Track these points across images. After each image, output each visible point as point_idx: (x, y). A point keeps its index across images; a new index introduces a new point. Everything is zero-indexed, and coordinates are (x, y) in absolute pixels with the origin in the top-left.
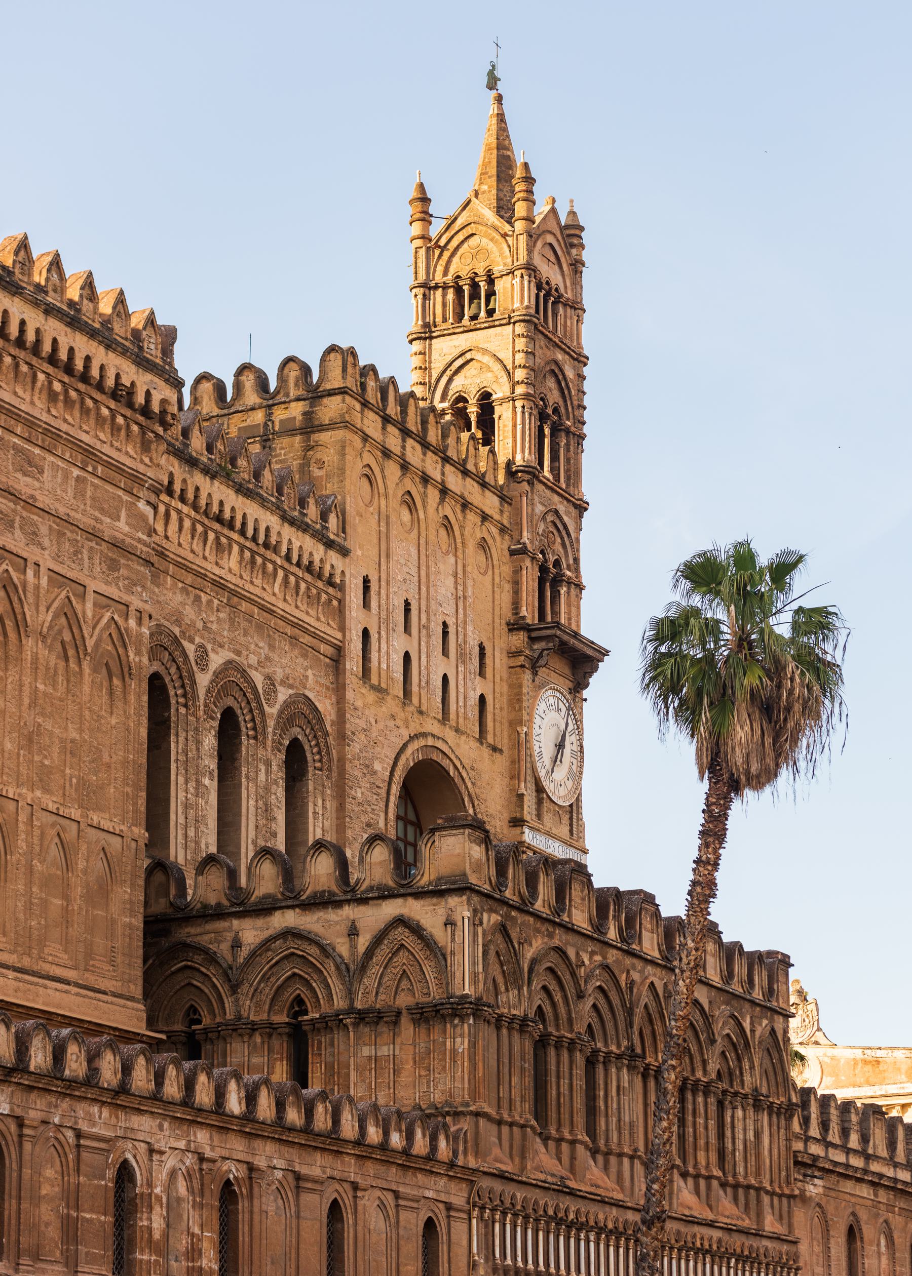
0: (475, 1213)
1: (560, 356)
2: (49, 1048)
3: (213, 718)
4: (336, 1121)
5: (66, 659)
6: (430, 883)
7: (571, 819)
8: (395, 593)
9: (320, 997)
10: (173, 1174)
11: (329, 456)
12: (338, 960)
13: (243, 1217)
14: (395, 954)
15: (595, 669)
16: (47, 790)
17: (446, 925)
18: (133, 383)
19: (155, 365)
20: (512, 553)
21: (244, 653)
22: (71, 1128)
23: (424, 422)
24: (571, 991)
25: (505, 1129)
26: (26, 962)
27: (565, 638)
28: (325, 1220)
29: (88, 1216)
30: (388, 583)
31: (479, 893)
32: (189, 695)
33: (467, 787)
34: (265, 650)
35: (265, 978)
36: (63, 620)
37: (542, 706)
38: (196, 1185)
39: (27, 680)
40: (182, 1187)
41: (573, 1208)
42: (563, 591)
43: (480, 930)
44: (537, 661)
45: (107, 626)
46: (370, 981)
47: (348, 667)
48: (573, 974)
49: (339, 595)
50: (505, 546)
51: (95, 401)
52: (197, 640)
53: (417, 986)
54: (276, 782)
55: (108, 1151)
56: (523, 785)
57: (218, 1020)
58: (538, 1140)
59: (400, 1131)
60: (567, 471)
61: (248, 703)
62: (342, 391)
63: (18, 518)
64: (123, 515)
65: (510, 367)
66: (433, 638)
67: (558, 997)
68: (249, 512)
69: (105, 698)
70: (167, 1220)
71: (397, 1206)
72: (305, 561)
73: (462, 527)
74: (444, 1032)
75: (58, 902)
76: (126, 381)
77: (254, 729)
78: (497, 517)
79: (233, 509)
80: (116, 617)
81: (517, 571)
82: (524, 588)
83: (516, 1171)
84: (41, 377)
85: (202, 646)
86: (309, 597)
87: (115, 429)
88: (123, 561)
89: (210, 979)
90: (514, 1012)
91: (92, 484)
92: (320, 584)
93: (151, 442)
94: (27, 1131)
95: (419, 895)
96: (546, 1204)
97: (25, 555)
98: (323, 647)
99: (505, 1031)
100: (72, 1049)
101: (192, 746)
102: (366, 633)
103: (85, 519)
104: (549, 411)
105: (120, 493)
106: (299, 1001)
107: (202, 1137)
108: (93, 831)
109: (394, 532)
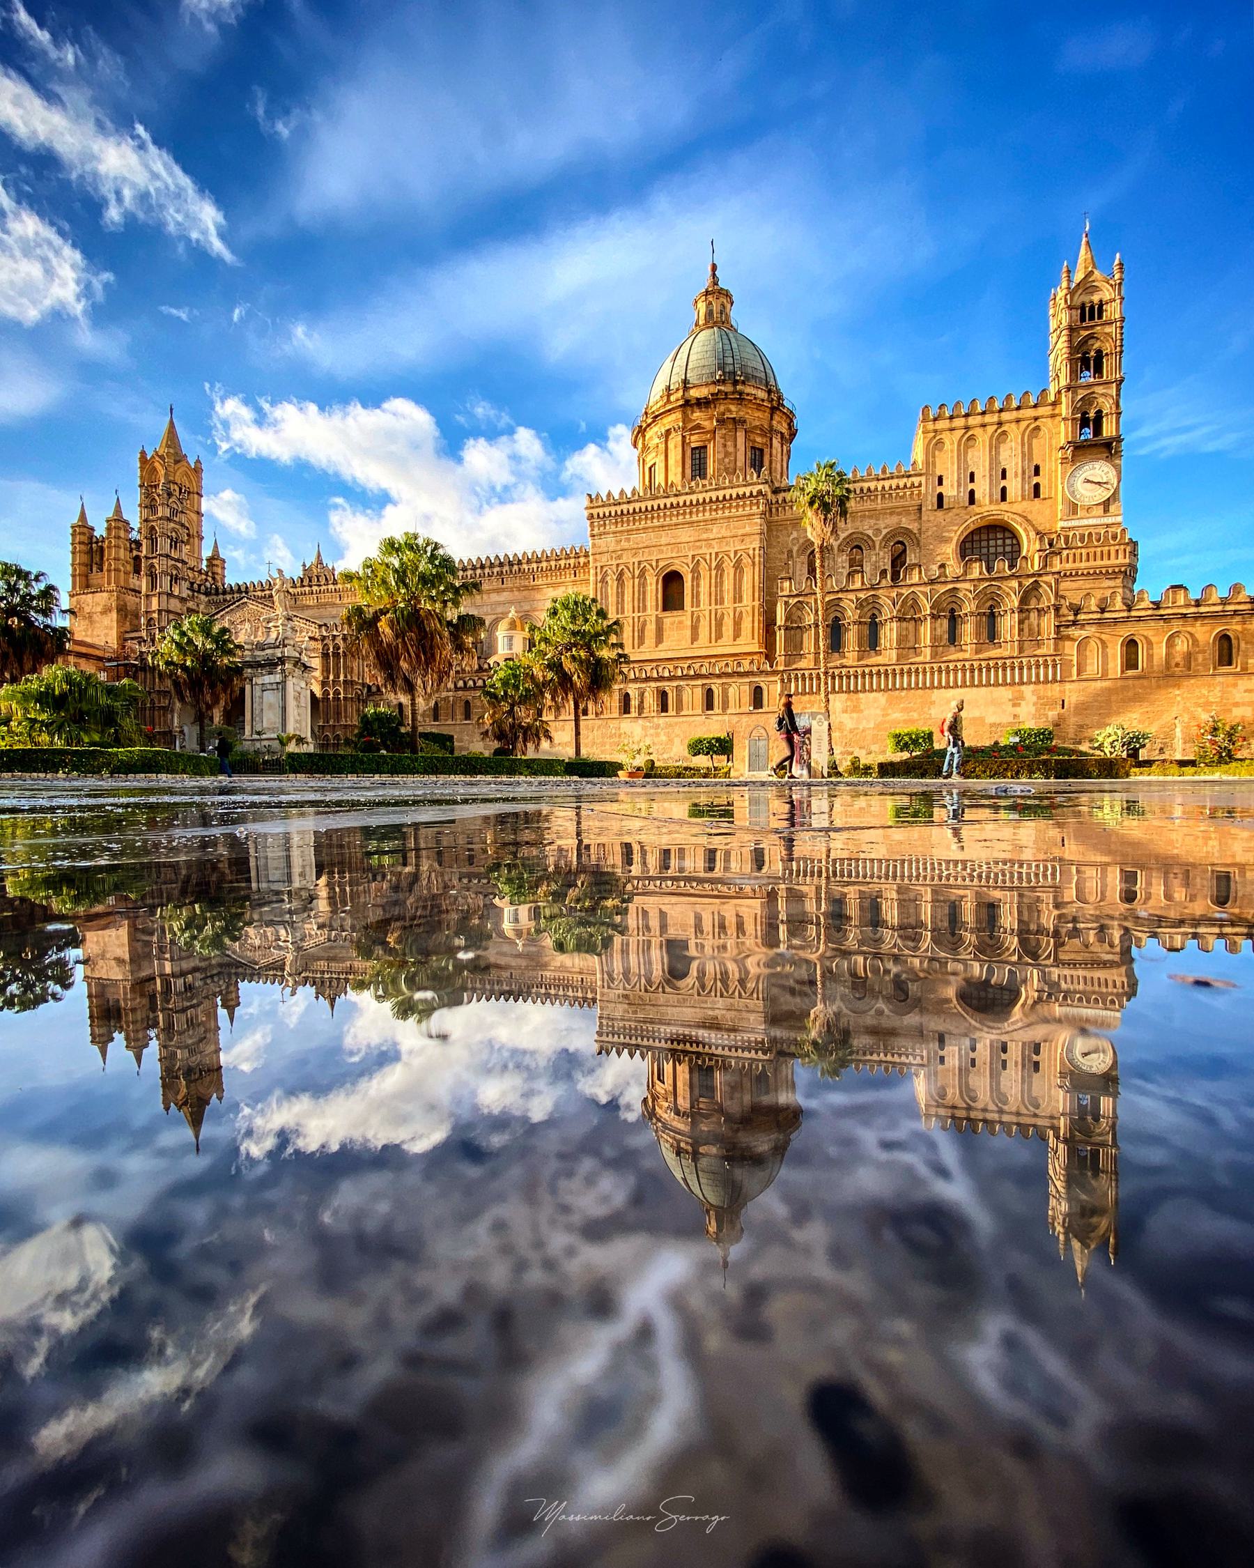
76: (741, 493)
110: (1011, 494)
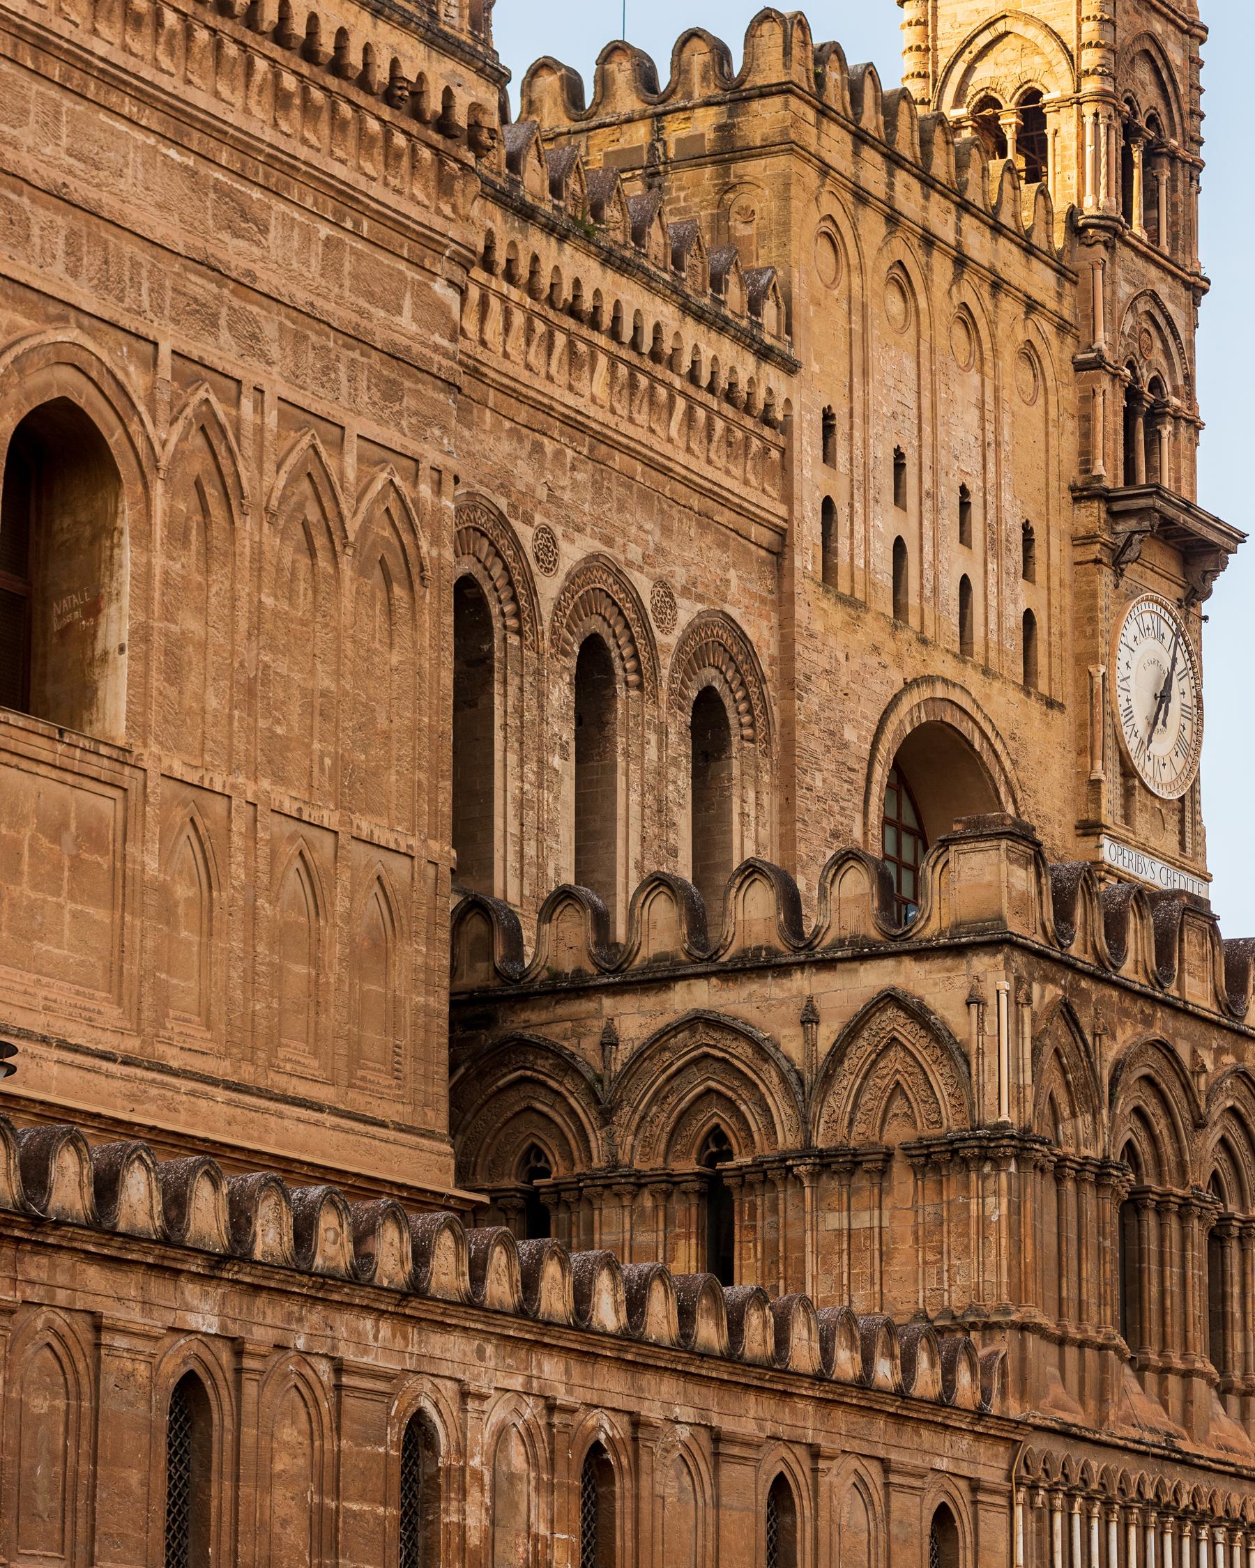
0: (1020, 1496)
1: (1158, 27)
2: (288, 1221)
3: (565, 653)
4: (782, 1341)
5: (312, 553)
6: (941, 934)
7: (1182, 821)
8: (878, 437)
9: (754, 1128)
10: (501, 1433)
11: (762, 201)
12: (784, 1065)
13: (622, 1507)
14: (881, 1054)
15: (1222, 565)
16: (280, 779)
17: (968, 1004)
18: (421, 77)
19: (459, 45)
20: (1079, 367)
21: (620, 541)
22: (325, 1356)
23: (926, 143)
24: (1183, 1116)
25: (1071, 1353)
26: (247, 1074)
27: (1171, 512)
28: (763, 1510)
29: (355, 1507)
30: (866, 419)
31: (1025, 949)
32: (524, 614)
33: (1003, 769)
34: (655, 537)
35: (659, 1098)
36: (306, 486)
37: (1130, 630)
38: (543, 1452)
39: (244, 590)
40: (517, 1457)
41: (1187, 1487)
42: (1167, 430)
43: (1027, 1012)
44: (1123, 552)
45: (382, 495)
46: (839, 1100)
47: (798, 563)
48: (1187, 1087)
49: (781, 441)
50: (1067, 355)
51: (356, 107)
52: (538, 519)
53: (920, 1110)
54: (675, 762)
55: (389, 1395)
56: (1099, 764)
57: (579, 1169)
58: (1128, 1370)
59: (892, 1357)
60: (1172, 225)
61: (627, 626)
62: (784, 89)
63: (224, 311)
64: (407, 303)
65: (1072, 46)
66: (944, 513)
67: (1161, 1126)
68: (624, 298)
69: (380, 619)
70: (492, 1512)
71: (887, 1485)
72: (723, 383)
73: (992, 323)
74: (967, 1187)
75: (301, 969)
76: (409, 73)
77: (638, 671)
78: (1052, 304)
79: (597, 294)
80: (397, 481)
81: (1088, 399)
82: (1099, 427)
83: (1090, 1425)
84: (261, 65)
85: (545, 530)
86: (730, 444)
87: (391, 156)
88: (408, 384)
89: (565, 1099)
90: (1086, 1152)
91: (354, 251)
92: (749, 422)
93: (454, 178)
94: (248, 1363)
95: (922, 953)
96: (1141, 1481)
97: (237, 373)
98: (755, 531)
99: (1070, 1186)
100: (328, 1221)
101: (531, 701)
102: (828, 506)
103: (341, 312)
104: (1141, 121)
105: (402, 266)
106: (717, 1135)
107: (551, 1369)
108: (362, 847)
109: (875, 332)
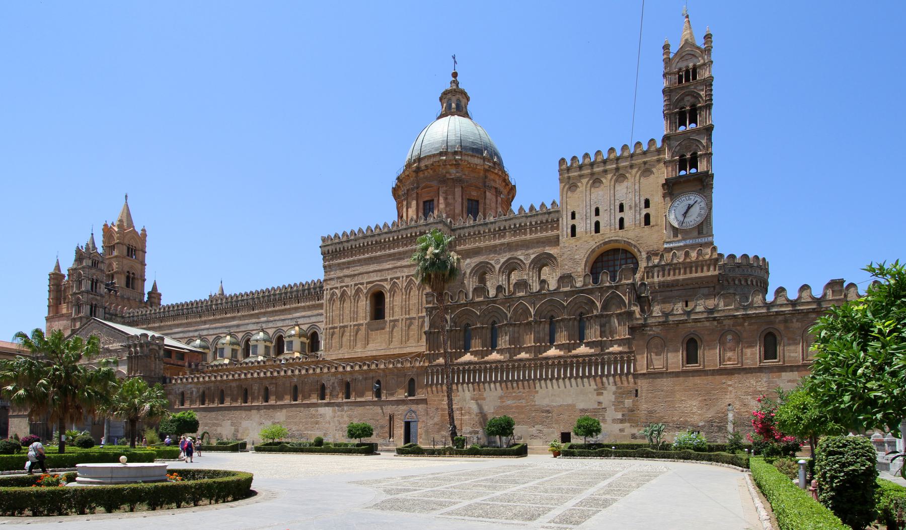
110: (626, 223)
